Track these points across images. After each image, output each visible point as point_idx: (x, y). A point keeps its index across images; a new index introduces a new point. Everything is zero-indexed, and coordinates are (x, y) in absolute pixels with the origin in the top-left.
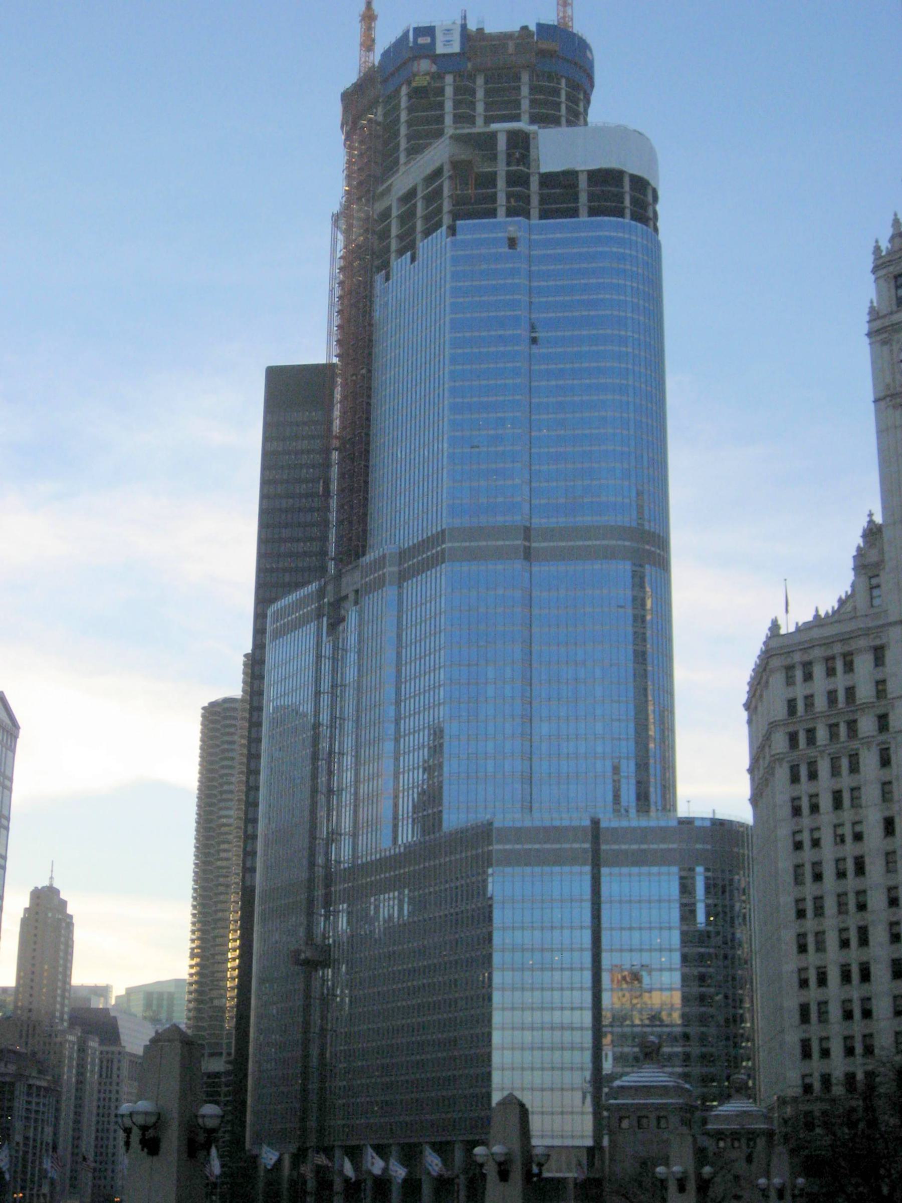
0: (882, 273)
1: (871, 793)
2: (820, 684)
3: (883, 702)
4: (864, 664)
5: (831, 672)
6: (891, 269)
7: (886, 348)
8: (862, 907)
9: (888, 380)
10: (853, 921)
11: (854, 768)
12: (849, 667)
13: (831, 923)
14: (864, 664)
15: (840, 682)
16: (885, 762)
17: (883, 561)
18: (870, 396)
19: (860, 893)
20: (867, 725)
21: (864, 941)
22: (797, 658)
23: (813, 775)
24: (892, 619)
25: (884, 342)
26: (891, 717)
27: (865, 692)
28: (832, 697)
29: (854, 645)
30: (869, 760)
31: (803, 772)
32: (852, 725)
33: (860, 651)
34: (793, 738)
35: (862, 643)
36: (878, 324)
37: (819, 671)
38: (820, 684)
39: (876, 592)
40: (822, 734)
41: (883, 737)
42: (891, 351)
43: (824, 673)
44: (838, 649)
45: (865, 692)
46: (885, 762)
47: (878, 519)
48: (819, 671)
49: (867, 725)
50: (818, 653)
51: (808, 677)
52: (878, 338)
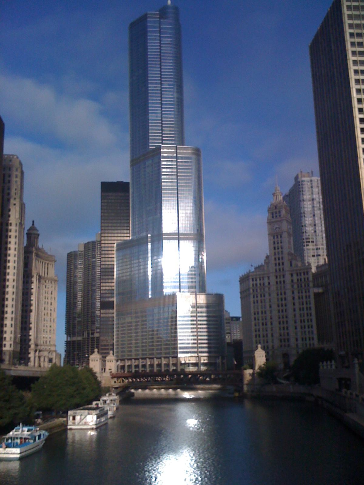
1: (267, 300)
4: (266, 279)
5: (260, 280)
12: (263, 279)
13: (261, 321)
14: (266, 279)
15: (262, 282)
16: (270, 295)
18: (267, 233)
19: (266, 317)
20: (267, 289)
21: (266, 324)
22: (254, 277)
23: (257, 297)
25: (270, 224)
27: (266, 284)
28: (260, 284)
30: (267, 295)
31: (255, 296)
32: (264, 289)
34: (253, 291)
38: (258, 282)
45: (266, 284)
46: (270, 295)
47: (269, 254)
49: (267, 289)
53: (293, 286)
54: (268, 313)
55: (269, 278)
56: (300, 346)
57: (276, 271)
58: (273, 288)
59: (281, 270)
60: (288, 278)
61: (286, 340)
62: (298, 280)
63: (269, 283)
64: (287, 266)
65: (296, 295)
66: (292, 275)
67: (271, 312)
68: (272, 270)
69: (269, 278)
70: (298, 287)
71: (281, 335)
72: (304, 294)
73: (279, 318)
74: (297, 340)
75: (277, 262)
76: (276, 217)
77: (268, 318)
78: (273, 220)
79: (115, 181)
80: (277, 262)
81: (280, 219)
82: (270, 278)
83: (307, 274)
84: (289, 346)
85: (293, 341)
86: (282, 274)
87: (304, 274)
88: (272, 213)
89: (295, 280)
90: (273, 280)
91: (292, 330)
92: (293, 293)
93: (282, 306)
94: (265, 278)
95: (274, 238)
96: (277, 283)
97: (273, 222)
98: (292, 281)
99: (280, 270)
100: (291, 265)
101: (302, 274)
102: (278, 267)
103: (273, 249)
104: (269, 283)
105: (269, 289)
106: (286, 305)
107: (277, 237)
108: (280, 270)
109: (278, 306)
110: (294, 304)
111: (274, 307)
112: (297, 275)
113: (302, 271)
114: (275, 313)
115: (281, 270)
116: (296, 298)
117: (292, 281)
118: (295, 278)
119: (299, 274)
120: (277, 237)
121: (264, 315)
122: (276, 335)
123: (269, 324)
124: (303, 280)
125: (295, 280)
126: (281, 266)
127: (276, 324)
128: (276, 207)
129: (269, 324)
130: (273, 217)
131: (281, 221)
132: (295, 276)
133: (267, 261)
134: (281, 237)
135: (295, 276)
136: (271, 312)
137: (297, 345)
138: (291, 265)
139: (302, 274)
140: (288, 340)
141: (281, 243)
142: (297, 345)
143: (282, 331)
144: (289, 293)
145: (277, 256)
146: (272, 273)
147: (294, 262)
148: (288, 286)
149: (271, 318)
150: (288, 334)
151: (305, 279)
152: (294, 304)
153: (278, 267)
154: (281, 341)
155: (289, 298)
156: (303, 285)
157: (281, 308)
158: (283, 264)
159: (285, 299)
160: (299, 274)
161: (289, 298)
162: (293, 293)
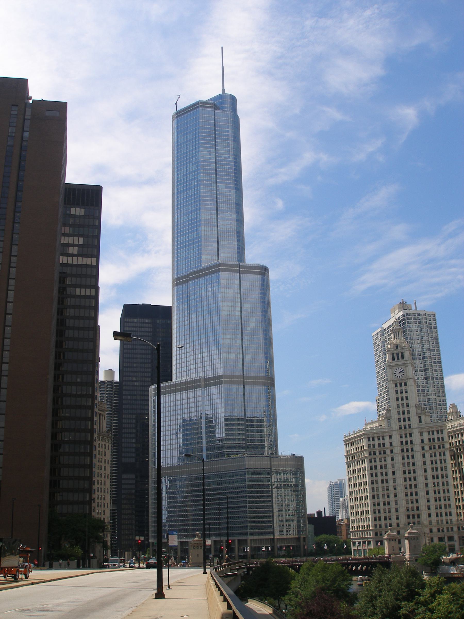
0: (389, 352)
1: (389, 466)
2: (376, 442)
3: (391, 447)
4: (387, 438)
5: (379, 439)
8: (388, 490)
9: (391, 377)
10: (386, 492)
11: (385, 461)
12: (383, 439)
13: (381, 493)
14: (387, 438)
16: (392, 459)
17: (391, 417)
20: (388, 452)
23: (375, 461)
24: (394, 429)
25: (390, 369)
26: (394, 451)
27: (388, 445)
28: (379, 445)
29: (384, 434)
30: (389, 459)
33: (386, 436)
35: (387, 434)
37: (376, 439)
38: (376, 442)
39: (389, 423)
40: (377, 453)
41: (392, 454)
42: (392, 371)
43: (377, 440)
44: (381, 435)
45: (388, 445)
46: (392, 459)
48: (376, 439)
49: (388, 452)
50: (376, 435)
51: (373, 439)
53: (423, 448)
54: (391, 482)
55: (390, 437)
56: (434, 522)
57: (400, 428)
58: (397, 450)
59: (407, 427)
60: (416, 438)
61: (416, 516)
62: (430, 439)
63: (391, 444)
64: (414, 422)
65: (428, 459)
66: (421, 434)
67: (394, 480)
68: (395, 425)
69: (390, 437)
70: (431, 449)
71: (408, 510)
72: (438, 458)
73: (406, 488)
74: (430, 515)
75: (402, 416)
76: (398, 358)
77: (391, 488)
78: (395, 363)
79: (100, 323)
80: (402, 416)
81: (402, 362)
82: (392, 437)
83: (442, 433)
84: (419, 523)
85: (424, 517)
86: (408, 432)
87: (438, 433)
89: (426, 440)
90: (396, 440)
91: (423, 504)
92: (424, 456)
93: (409, 473)
94: (385, 438)
95: (396, 386)
96: (402, 443)
98: (422, 441)
99: (405, 428)
100: (420, 421)
101: (435, 433)
102: (402, 423)
103: (396, 400)
104: (391, 444)
105: (392, 452)
106: (414, 472)
107: (401, 385)
108: (405, 428)
109: (405, 473)
110: (425, 471)
111: (399, 474)
112: (429, 434)
113: (435, 429)
114: (400, 482)
115: (407, 427)
116: (428, 462)
117: (422, 441)
118: (426, 437)
119: (431, 433)
120: (401, 385)
121: (385, 484)
122: (402, 510)
123: (392, 496)
124: (436, 440)
125: (426, 440)
126: (407, 423)
127: (401, 495)
128: (397, 347)
129: (392, 496)
130: (393, 359)
131: (405, 365)
132: (425, 434)
133: (388, 415)
134: (405, 384)
135: (425, 434)
136: (394, 480)
137: (430, 522)
138: (420, 421)
139: (435, 433)
140: (418, 516)
141: (406, 392)
142: (430, 522)
143: (410, 505)
144: (418, 456)
145: (401, 410)
146: (396, 430)
147: (423, 418)
148: (417, 448)
149: (395, 489)
150: (418, 509)
151: (438, 438)
152: (425, 471)
153: (402, 423)
154: (408, 517)
155: (419, 464)
156: (437, 447)
157: (407, 475)
158: (409, 420)
159: (414, 464)
160: (431, 433)
161: (419, 464)
162: (424, 456)
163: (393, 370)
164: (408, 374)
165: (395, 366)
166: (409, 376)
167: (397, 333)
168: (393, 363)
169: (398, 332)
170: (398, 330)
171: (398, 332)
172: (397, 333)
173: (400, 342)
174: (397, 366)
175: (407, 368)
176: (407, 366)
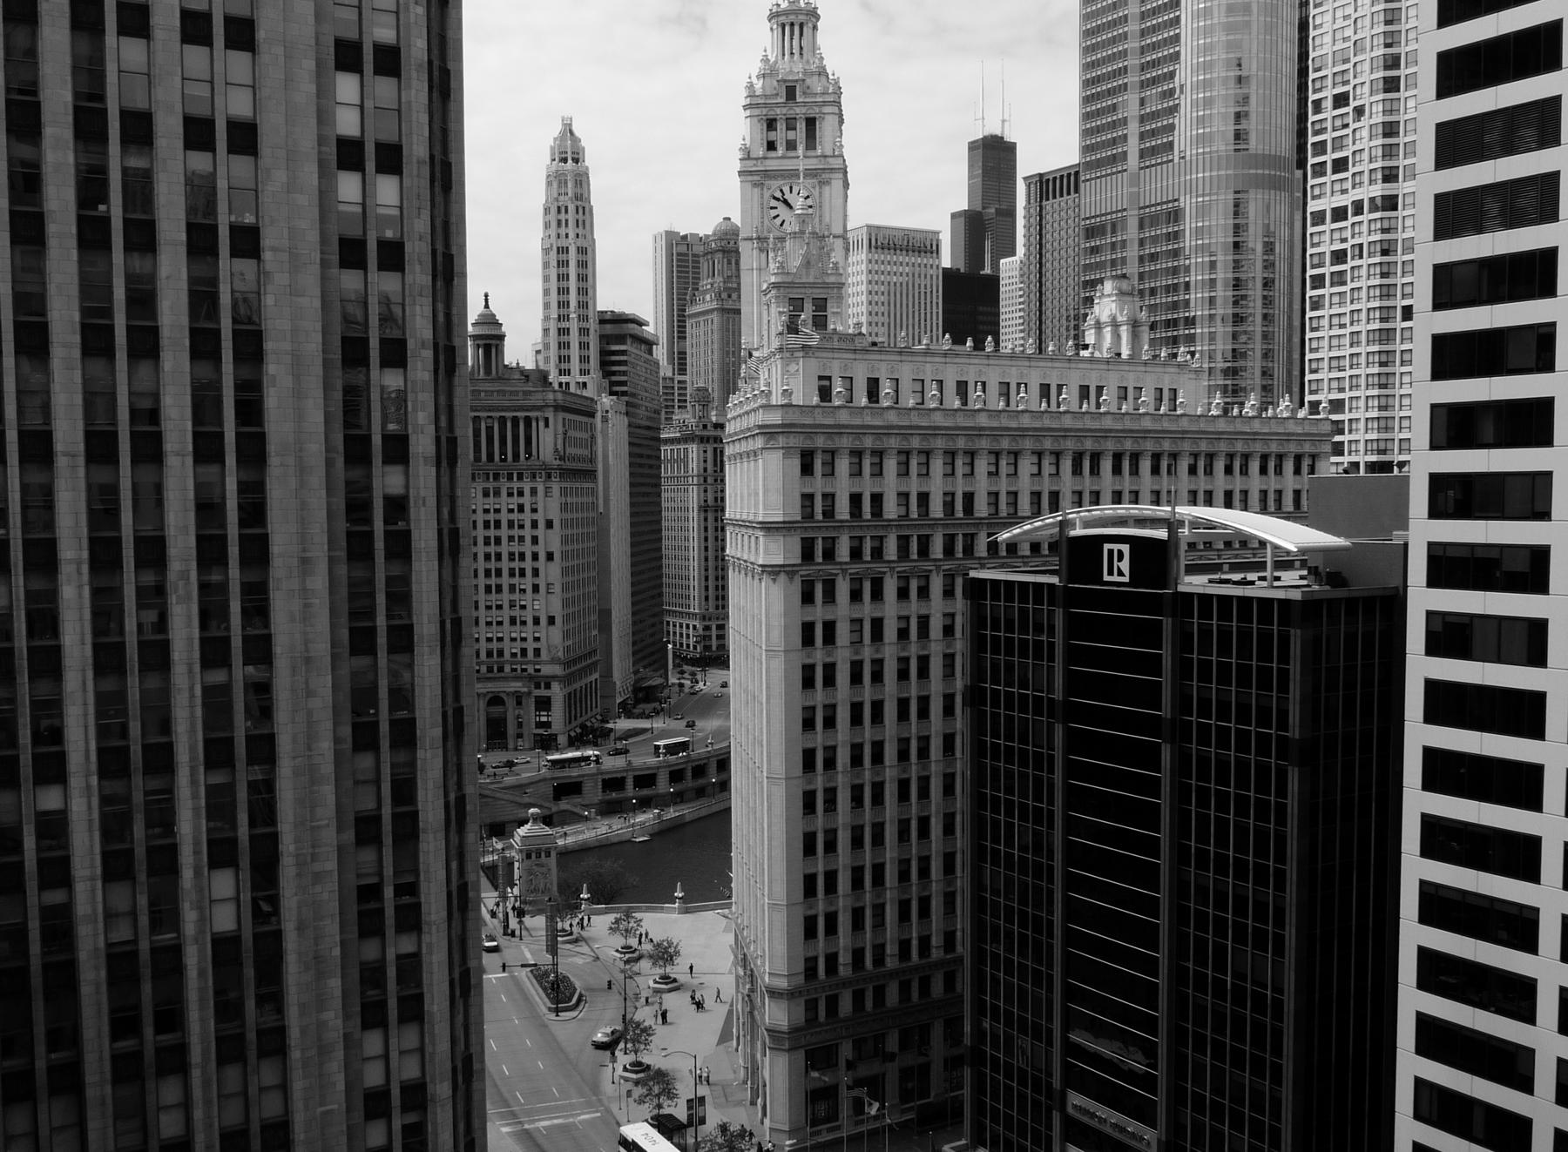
0: (757, 112)
6: (765, 111)
7: (757, 191)
25: (755, 185)
36: (750, 165)
52: (750, 178)
78: (772, 165)
88: (771, 124)
97: (767, 174)
128: (791, 93)
163: (767, 194)
164: (827, 220)
165: (775, 178)
166: (829, 227)
167: (797, 29)
168: (768, 162)
169: (801, 26)
170: (802, 18)
171: (801, 26)
172: (797, 29)
173: (805, 73)
174: (783, 177)
175: (826, 189)
176: (828, 183)
